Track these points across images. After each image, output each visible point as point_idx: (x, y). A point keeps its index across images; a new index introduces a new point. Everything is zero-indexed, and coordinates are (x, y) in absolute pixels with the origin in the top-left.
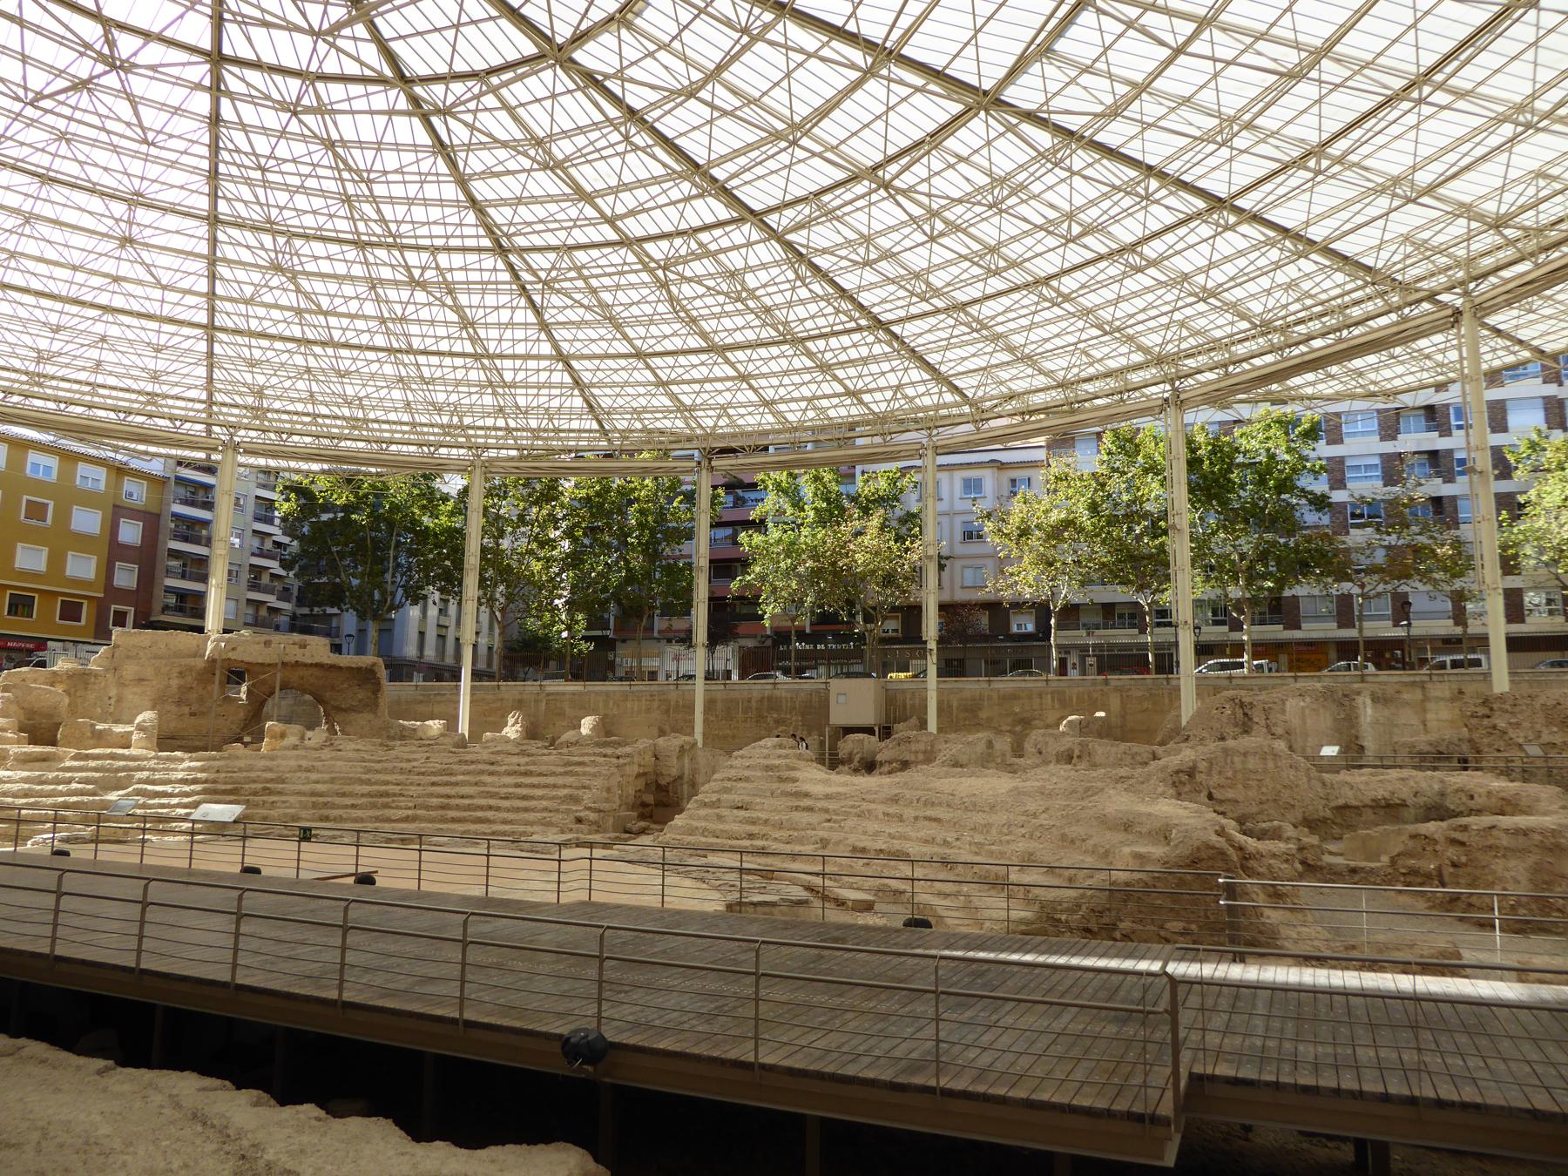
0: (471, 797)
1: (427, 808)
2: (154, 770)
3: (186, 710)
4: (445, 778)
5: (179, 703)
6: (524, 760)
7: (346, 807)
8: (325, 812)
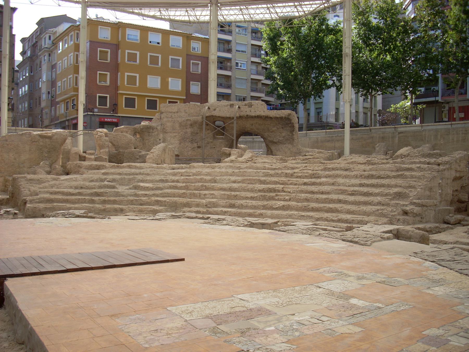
0: (328, 193)
1: (298, 201)
2: (148, 174)
3: (195, 145)
4: (313, 180)
5: (192, 141)
6: (368, 167)
7: (247, 198)
8: (233, 202)
